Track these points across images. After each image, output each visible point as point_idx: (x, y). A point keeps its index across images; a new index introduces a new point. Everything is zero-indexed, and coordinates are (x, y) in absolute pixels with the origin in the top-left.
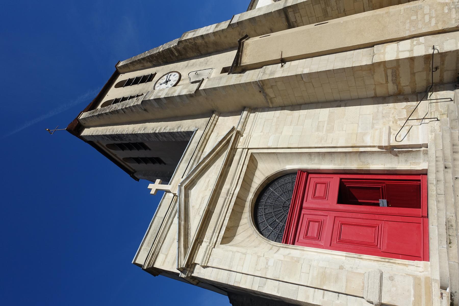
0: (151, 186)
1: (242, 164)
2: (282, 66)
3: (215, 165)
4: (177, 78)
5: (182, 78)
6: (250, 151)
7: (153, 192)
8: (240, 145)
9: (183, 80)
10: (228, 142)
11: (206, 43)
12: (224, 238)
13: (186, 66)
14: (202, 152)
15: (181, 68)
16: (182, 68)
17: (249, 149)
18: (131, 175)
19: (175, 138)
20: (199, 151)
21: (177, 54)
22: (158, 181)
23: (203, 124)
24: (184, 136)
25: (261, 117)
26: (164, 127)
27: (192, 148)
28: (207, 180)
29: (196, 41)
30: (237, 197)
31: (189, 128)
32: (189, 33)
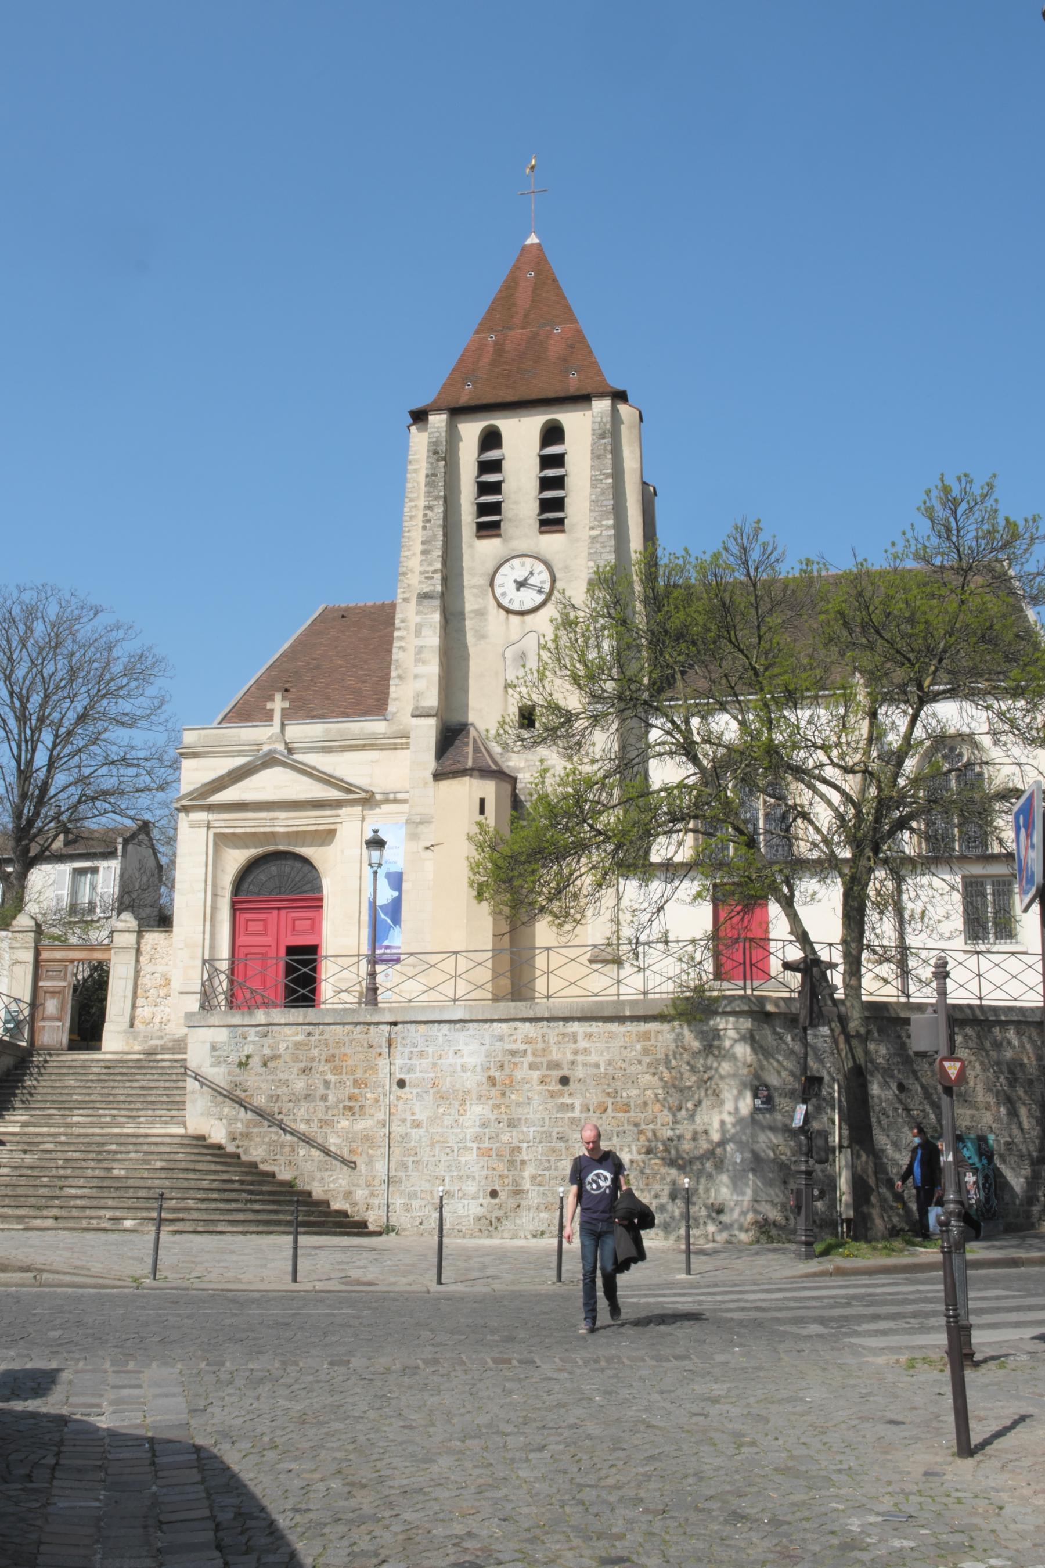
0: (278, 696)
5: (528, 618)
7: (269, 706)
8: (343, 811)
9: (523, 622)
10: (350, 792)
12: (223, 834)
20: (340, 746)
22: (286, 705)
30: (272, 833)
31: (395, 699)
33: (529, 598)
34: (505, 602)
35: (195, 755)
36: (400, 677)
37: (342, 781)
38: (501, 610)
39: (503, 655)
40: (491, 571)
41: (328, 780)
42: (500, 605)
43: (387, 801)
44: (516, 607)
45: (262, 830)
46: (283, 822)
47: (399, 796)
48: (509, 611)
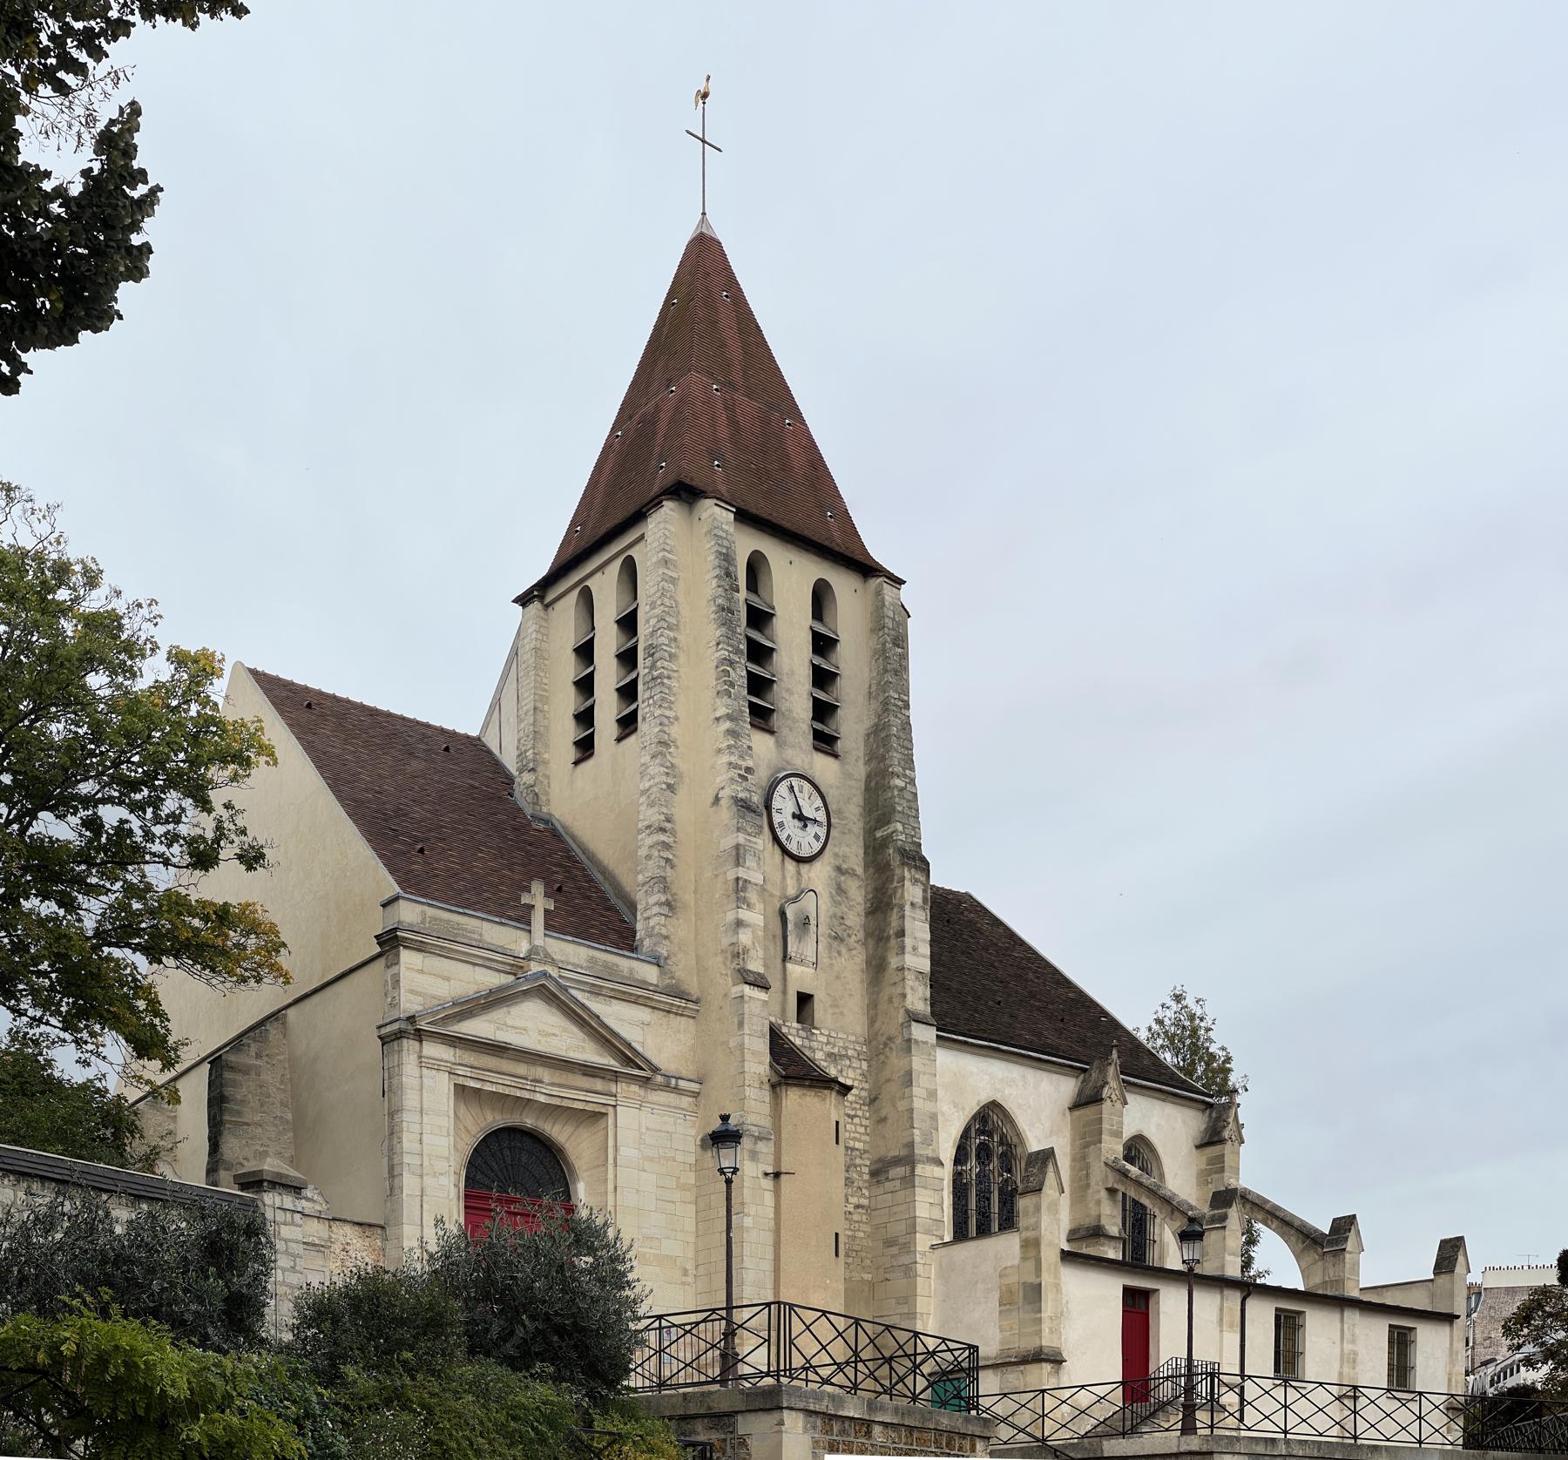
1: (588, 1099)
2: (766, 1174)
3: (584, 1042)
4: (805, 853)
5: (804, 868)
6: (610, 1109)
8: (621, 1088)
9: (799, 873)
10: (628, 1061)
11: (888, 938)
12: (464, 1087)
13: (839, 869)
14: (611, 997)
15: (836, 850)
16: (836, 855)
17: (615, 1106)
18: (536, 593)
19: (645, 888)
20: (613, 990)
21: (879, 834)
23: (673, 978)
24: (649, 918)
25: (679, 1121)
26: (671, 857)
27: (617, 966)
28: (556, 1031)
29: (895, 910)
32: (924, 884)
33: (804, 840)
34: (783, 837)
35: (420, 948)
36: (668, 904)
37: (629, 1046)
38: (776, 846)
39: (783, 914)
40: (765, 783)
41: (605, 1038)
42: (776, 839)
43: (666, 1087)
44: (792, 848)
45: (518, 1093)
46: (548, 1088)
47: (682, 1084)
48: (785, 852)
